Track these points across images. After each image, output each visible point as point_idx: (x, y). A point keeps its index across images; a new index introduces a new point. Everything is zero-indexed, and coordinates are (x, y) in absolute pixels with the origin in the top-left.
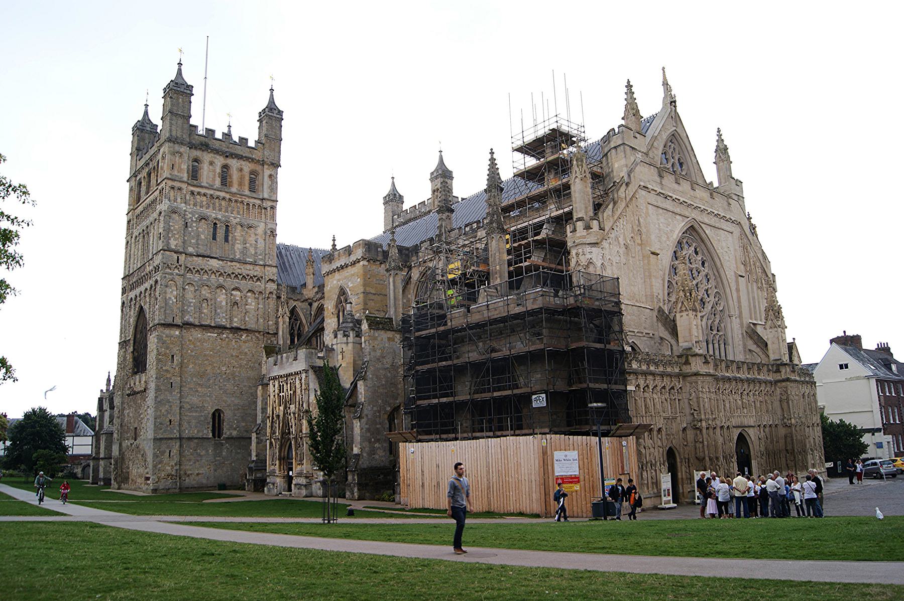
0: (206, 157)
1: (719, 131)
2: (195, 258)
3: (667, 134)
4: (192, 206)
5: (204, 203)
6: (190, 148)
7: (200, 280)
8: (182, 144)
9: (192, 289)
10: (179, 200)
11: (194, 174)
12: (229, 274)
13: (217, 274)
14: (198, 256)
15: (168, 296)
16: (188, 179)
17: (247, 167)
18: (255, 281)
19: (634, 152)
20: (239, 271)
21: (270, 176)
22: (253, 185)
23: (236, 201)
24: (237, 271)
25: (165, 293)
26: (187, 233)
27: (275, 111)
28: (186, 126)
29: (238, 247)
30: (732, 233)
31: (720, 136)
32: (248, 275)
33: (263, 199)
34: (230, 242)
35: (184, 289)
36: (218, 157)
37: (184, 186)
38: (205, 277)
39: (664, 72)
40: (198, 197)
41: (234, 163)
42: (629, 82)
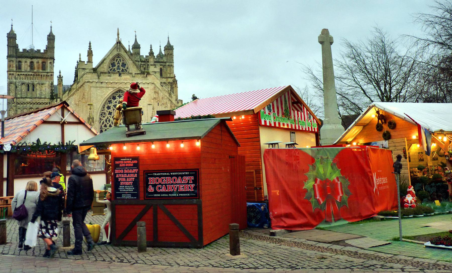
0: (23, 60)
1: (151, 46)
2: (20, 99)
3: (113, 56)
4: (19, 80)
5: (24, 78)
6: (16, 58)
7: (23, 107)
8: (13, 57)
9: (20, 110)
10: (13, 78)
11: (19, 68)
12: (34, 103)
13: (30, 104)
14: (21, 98)
15: (10, 114)
16: (16, 70)
17: (40, 61)
18: (45, 104)
19: (84, 70)
20: (39, 102)
21: (50, 63)
22: (44, 67)
23: (36, 75)
24: (37, 102)
25: (9, 113)
26: (17, 90)
27: (51, 37)
28: (14, 50)
29: (38, 92)
30: (148, 88)
31: (151, 47)
32: (42, 103)
33: (47, 73)
34: (35, 91)
35: (16, 111)
36: (28, 59)
37: (15, 73)
38: (25, 105)
39: (118, 30)
40: (21, 76)
41: (35, 61)
42: (90, 42)
